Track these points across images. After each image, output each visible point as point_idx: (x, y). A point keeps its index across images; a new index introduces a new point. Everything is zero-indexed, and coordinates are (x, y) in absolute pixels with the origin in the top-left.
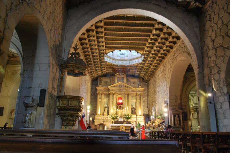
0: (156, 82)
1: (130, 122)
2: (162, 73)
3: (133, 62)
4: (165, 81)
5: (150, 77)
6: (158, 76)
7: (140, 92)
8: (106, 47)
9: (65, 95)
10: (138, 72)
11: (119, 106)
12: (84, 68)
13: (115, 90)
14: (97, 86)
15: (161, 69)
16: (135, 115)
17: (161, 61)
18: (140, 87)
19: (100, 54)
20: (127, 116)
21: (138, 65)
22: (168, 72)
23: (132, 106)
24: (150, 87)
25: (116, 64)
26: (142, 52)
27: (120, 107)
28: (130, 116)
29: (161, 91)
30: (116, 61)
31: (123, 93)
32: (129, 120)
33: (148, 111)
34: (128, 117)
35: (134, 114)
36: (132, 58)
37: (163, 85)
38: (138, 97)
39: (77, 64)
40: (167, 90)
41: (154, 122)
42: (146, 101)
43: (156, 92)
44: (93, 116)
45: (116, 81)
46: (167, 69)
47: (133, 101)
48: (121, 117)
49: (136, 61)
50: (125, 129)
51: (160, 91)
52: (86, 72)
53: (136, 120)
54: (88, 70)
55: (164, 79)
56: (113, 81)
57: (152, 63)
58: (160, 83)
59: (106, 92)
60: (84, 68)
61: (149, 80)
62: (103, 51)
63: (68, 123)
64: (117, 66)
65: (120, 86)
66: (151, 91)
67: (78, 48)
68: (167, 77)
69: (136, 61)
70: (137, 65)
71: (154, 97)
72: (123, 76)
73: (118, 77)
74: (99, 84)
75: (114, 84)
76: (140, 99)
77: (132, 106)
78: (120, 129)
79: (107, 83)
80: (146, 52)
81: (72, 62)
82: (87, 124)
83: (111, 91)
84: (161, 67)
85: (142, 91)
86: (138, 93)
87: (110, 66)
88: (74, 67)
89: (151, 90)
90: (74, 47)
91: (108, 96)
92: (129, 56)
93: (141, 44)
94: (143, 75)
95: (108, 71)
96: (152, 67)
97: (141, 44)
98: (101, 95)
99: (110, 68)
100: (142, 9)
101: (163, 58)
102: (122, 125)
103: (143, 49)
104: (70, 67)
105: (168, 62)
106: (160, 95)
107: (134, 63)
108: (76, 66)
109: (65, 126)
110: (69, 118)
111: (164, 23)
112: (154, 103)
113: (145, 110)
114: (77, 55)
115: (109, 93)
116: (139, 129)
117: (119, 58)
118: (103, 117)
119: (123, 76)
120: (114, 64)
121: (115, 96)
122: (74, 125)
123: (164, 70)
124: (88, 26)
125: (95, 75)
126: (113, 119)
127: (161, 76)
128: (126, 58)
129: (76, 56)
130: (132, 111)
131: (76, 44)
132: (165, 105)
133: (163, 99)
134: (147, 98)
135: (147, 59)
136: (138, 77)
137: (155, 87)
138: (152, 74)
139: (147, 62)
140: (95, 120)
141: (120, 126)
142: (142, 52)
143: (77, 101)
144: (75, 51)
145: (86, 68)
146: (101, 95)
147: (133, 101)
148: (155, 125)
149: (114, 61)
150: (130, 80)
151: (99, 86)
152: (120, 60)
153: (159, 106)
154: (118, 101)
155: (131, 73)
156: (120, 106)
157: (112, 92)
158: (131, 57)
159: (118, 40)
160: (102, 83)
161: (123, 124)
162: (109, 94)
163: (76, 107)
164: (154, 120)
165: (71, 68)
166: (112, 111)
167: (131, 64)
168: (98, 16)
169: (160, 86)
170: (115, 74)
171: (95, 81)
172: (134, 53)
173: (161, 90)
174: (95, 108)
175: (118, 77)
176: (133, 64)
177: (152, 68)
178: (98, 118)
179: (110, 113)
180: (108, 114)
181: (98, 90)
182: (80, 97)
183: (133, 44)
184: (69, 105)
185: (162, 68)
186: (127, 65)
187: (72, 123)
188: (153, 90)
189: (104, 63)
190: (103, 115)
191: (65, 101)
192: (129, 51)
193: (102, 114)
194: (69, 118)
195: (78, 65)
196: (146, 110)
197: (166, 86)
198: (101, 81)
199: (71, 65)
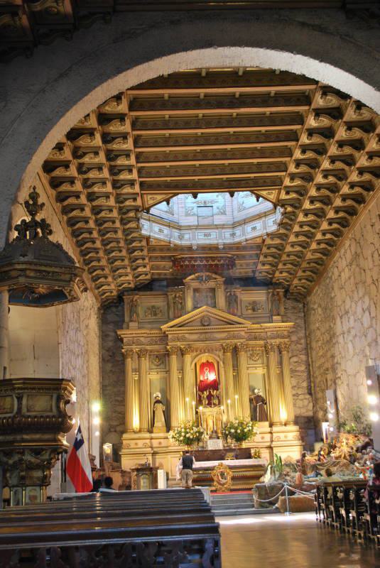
0: (332, 298)
1: (249, 449)
2: (351, 264)
4: (364, 296)
5: (311, 282)
6: (340, 276)
7: (278, 337)
9: (8, 377)
10: (267, 267)
11: (206, 394)
12: (67, 277)
13: (187, 336)
15: (346, 252)
16: (267, 424)
17: (344, 223)
18: (277, 322)
19: (124, 210)
20: (236, 429)
21: (264, 241)
22: (373, 261)
23: (252, 389)
24: (312, 318)
25: (185, 243)
26: (273, 197)
27: (210, 397)
28: (246, 430)
29: (353, 332)
30: (183, 232)
31: (217, 344)
32: (245, 445)
33: (311, 404)
34: (239, 431)
35: (261, 420)
36: (239, 216)
37: (359, 310)
38: (274, 357)
39: (41, 265)
40: (371, 326)
41: (334, 447)
42: (303, 368)
43: (334, 334)
44: (113, 436)
45: (189, 304)
46: (368, 253)
47: (255, 373)
48: (214, 435)
50: (233, 478)
51: (349, 332)
52: (77, 289)
53: (272, 441)
54: (83, 282)
55: (360, 285)
56: (180, 306)
57: (313, 231)
58: (348, 301)
59: (156, 347)
60: (67, 277)
61: (309, 292)
62: (135, 200)
63: (23, 478)
64: (190, 248)
65: (204, 322)
66: (318, 333)
67: (43, 204)
68: (369, 281)
69: (254, 228)
70: (259, 241)
71: (329, 354)
72: (211, 284)
73: (196, 290)
74: (127, 319)
75: (181, 316)
76: (281, 363)
77: (252, 389)
78: (215, 478)
79: (155, 315)
80: (287, 193)
81: (22, 259)
82: (93, 469)
83: (174, 341)
84: (347, 243)
85: (286, 333)
86: (273, 341)
87: (161, 250)
88: (32, 274)
89: (318, 329)
90: (27, 203)
91: (162, 359)
92: (228, 210)
94: (285, 274)
95: (158, 268)
96: (314, 246)
98: (139, 357)
99: (163, 258)
100: (261, 47)
101: (352, 212)
102: (221, 465)
103: (276, 183)
104: (17, 277)
105: (369, 227)
106: (350, 345)
107: (249, 236)
108: (40, 271)
109: (14, 486)
110: (28, 457)
111: (343, 90)
112: (329, 377)
113: (300, 403)
114: (39, 230)
115: (167, 351)
116: (281, 474)
117: (192, 221)
118: (151, 439)
119: (211, 284)
120: (178, 242)
121: (188, 358)
122: (44, 482)
123: (356, 256)
124: (72, 119)
125: (112, 288)
126: (188, 442)
127: (349, 278)
128: (218, 220)
129: (37, 234)
130: (254, 411)
131: (34, 188)
132: (369, 382)
133: (361, 361)
134: (304, 357)
135: (293, 218)
136: (268, 283)
137: (329, 317)
138: (318, 271)
139: (296, 228)
140: (124, 451)
141: (212, 469)
143: (52, 396)
144: (33, 213)
145: (76, 275)
147: (255, 373)
148: (340, 457)
149: (176, 233)
150: (238, 294)
151: (128, 328)
152: (198, 227)
153: (348, 385)
154: (201, 379)
155: (240, 270)
156: (208, 393)
157: (179, 344)
158: (236, 213)
159: (186, 157)
160: (138, 315)
161: (222, 458)
163: (48, 417)
164: (332, 439)
165: (22, 280)
166: (183, 414)
167: (237, 240)
168: (105, 85)
169: (347, 312)
170: (185, 278)
171: (114, 309)
172: (245, 199)
173: (353, 328)
174: (119, 409)
175: (196, 290)
176: (247, 240)
177: (315, 251)
178: (132, 443)
179: (174, 423)
180: (168, 427)
181: (125, 340)
182: (63, 380)
183: (241, 168)
184: (24, 410)
185: (350, 245)
186: (224, 244)
187: (38, 474)
188: (323, 330)
189: (141, 241)
190: (151, 432)
191: (8, 399)
192: (227, 195)
193: (145, 426)
194: (28, 457)
195: (46, 266)
196: (306, 402)
197: (367, 313)
198: (133, 306)
199: (21, 270)
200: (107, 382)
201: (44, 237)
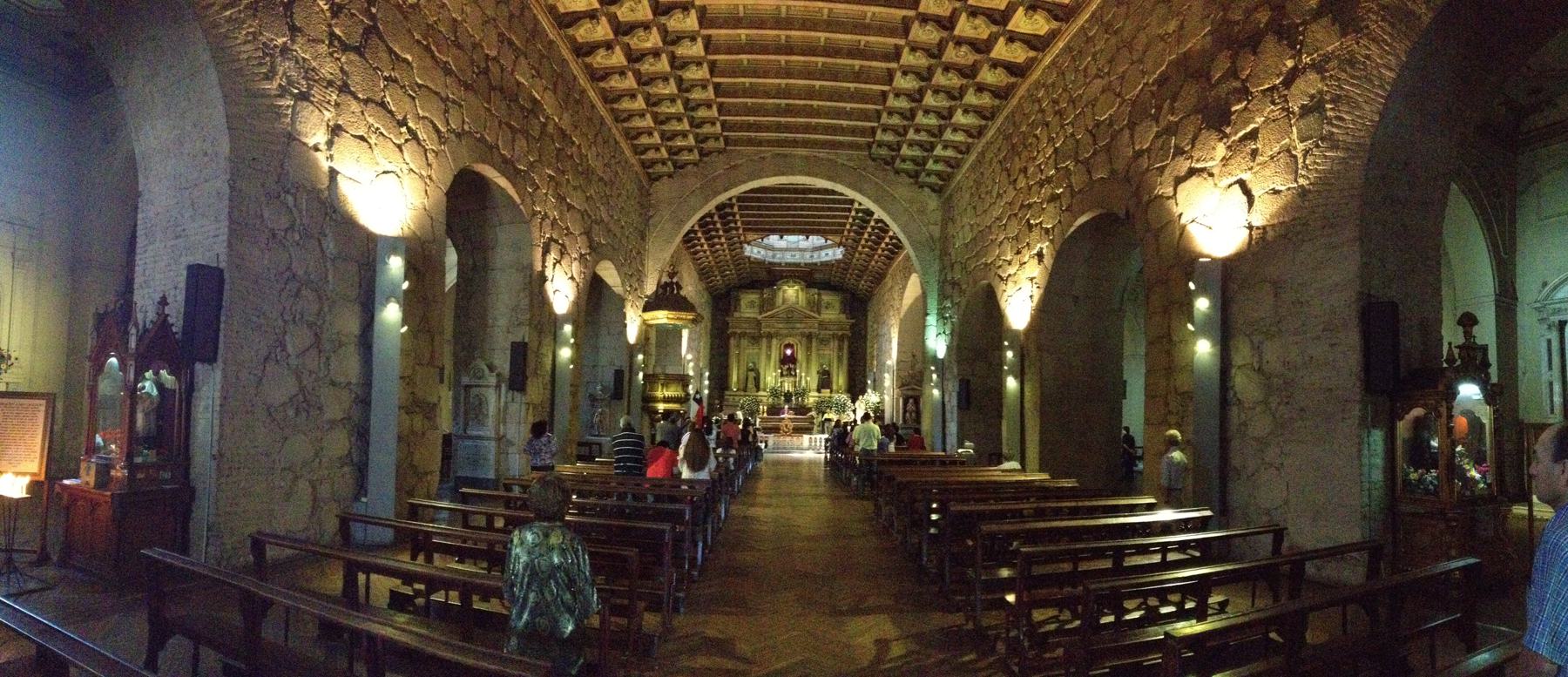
3: (819, 257)
8: (744, 230)
14: (728, 315)
25: (775, 260)
27: (789, 369)
49: (827, 254)
64: (780, 264)
93: (842, 217)
97: (842, 217)
120: (771, 260)
121: (774, 342)
142: (837, 239)
146: (740, 338)
152: (787, 250)
156: (788, 363)
162: (761, 337)
167: (814, 261)
172: (816, 240)
190: (745, 390)
200: (714, 353)
201: (678, 293)
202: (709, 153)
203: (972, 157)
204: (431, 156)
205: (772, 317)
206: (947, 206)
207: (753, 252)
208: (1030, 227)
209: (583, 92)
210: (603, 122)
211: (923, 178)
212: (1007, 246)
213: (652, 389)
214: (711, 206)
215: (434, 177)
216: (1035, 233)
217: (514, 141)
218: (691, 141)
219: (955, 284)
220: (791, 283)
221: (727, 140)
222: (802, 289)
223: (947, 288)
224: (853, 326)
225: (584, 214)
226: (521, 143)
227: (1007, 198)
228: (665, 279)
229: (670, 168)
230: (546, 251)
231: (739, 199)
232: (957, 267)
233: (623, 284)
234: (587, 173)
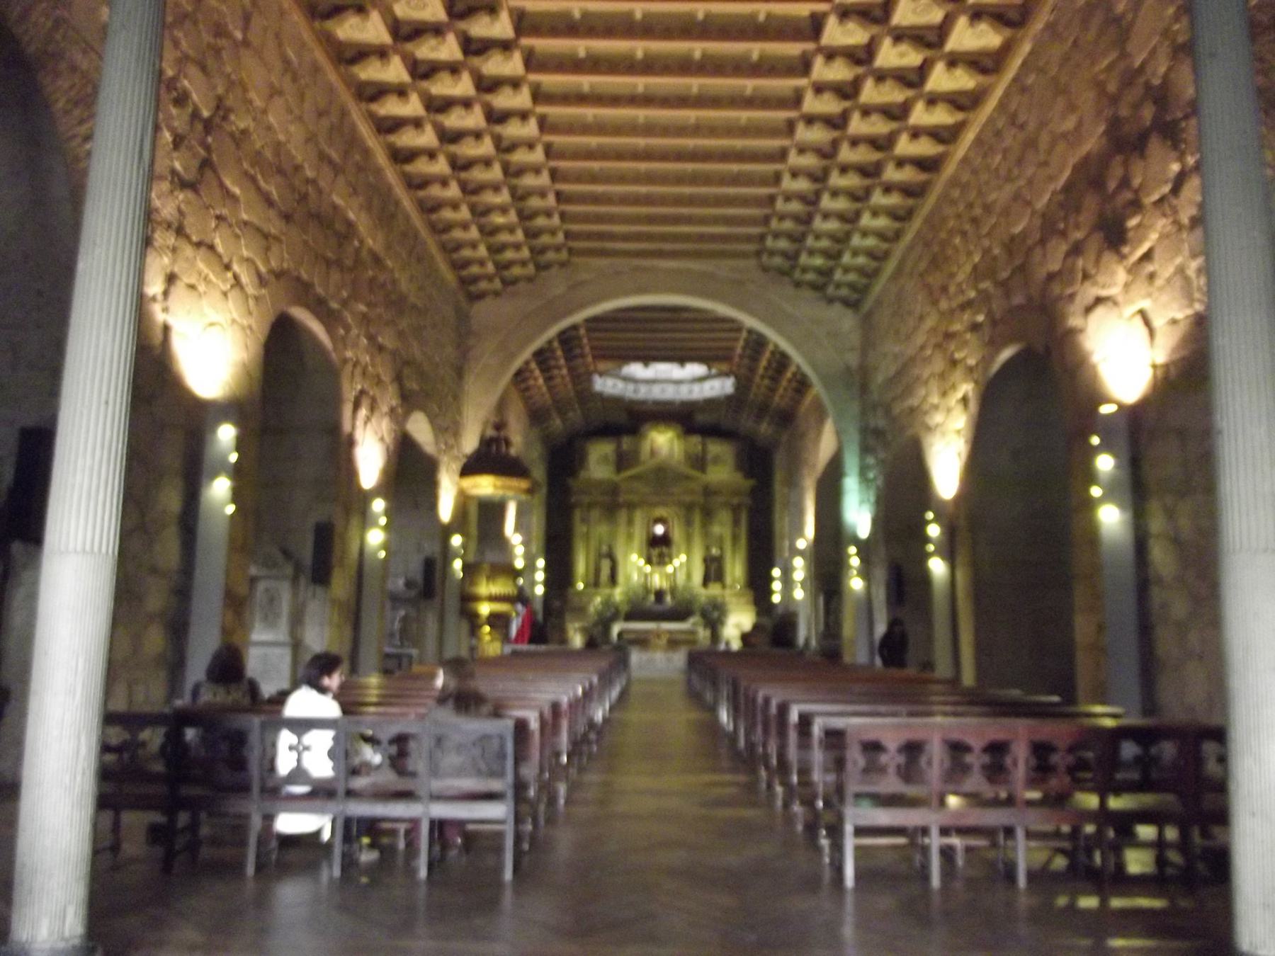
3: (702, 390)
8: (595, 357)
142: (725, 367)
149: (631, 387)
155: (701, 418)
156: (658, 548)
179: (621, 578)
202: (547, 266)
203: (890, 267)
204: (251, 302)
205: (632, 478)
206: (867, 322)
207: (606, 385)
208: (954, 363)
209: (397, 203)
210: (416, 235)
211: (831, 290)
212: (934, 386)
213: (473, 583)
214: (553, 331)
215: (254, 326)
216: (958, 374)
217: (328, 273)
218: (525, 253)
219: (878, 433)
220: (662, 428)
221: (571, 251)
222: (679, 437)
223: (872, 439)
224: (753, 492)
225: (394, 354)
226: (335, 276)
227: (930, 323)
228: (490, 432)
229: (497, 284)
230: (356, 406)
231: (588, 321)
232: (880, 412)
233: (437, 443)
234: (398, 304)
